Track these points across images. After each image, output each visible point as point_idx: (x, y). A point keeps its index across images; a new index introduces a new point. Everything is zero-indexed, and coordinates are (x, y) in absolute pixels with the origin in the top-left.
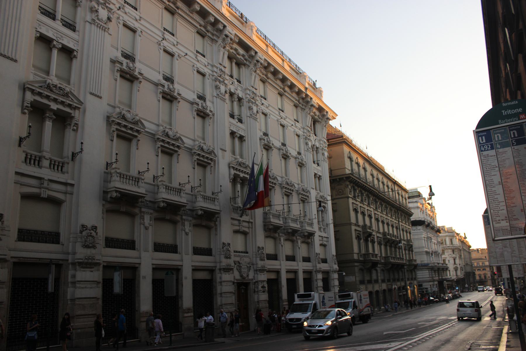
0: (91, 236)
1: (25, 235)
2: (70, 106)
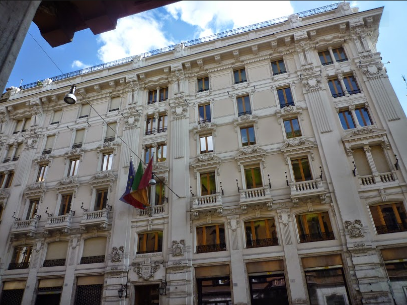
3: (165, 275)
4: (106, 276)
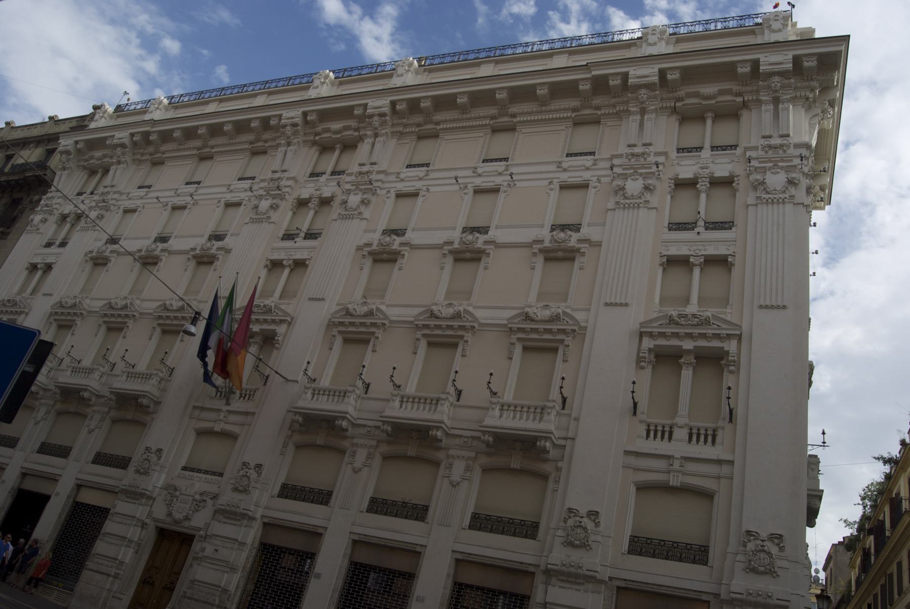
0: (763, 551)
1: (640, 546)
2: (717, 336)
4: (539, 579)
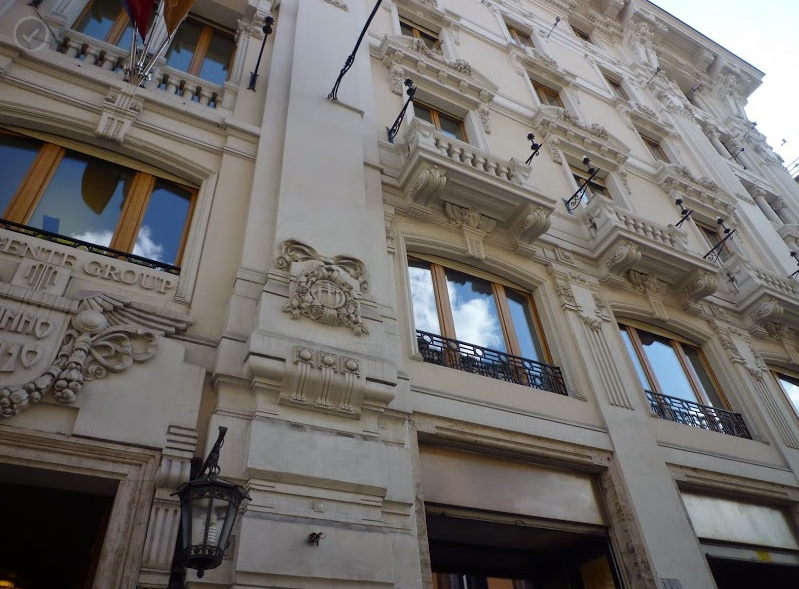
0: (329, 278)
3: (191, 420)
